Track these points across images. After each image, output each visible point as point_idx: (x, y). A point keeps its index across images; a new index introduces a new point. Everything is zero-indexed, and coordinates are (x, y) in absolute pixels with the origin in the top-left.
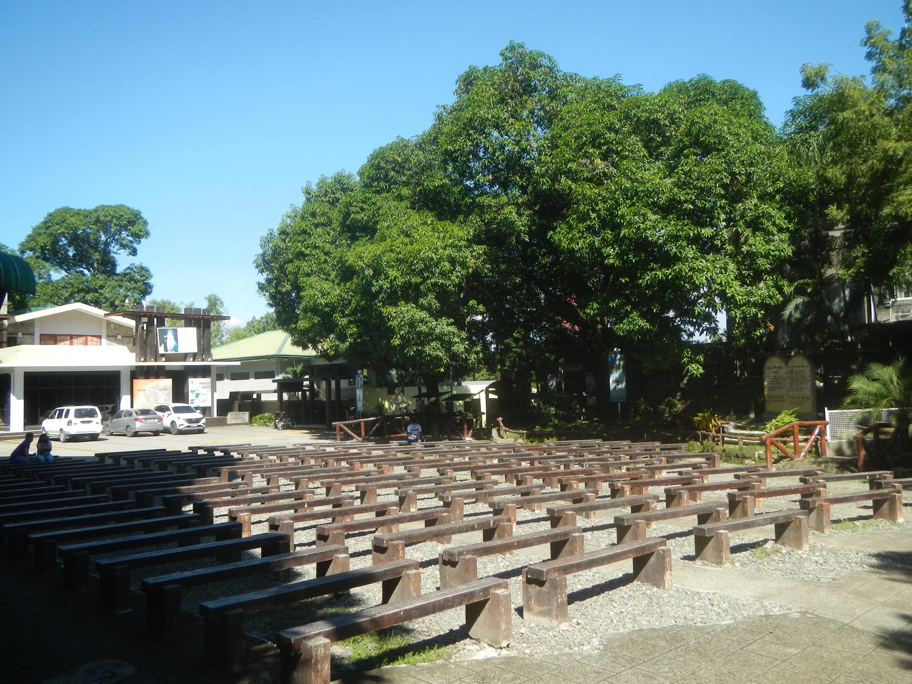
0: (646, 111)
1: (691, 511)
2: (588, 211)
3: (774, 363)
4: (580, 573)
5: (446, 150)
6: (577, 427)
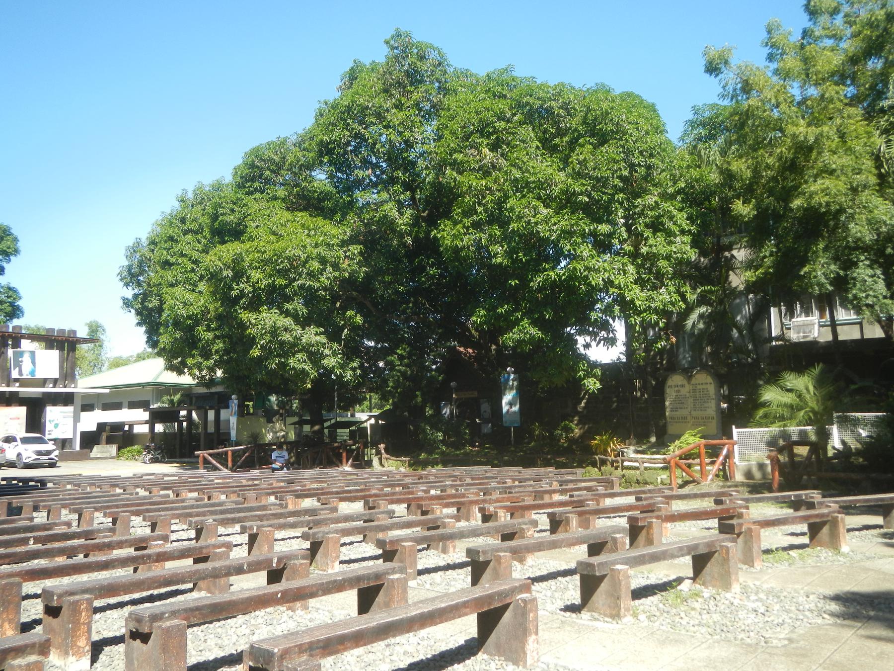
0: (539, 99)
1: (577, 538)
2: (474, 204)
3: (676, 380)
4: (398, 639)
5: (322, 141)
6: (466, 454)
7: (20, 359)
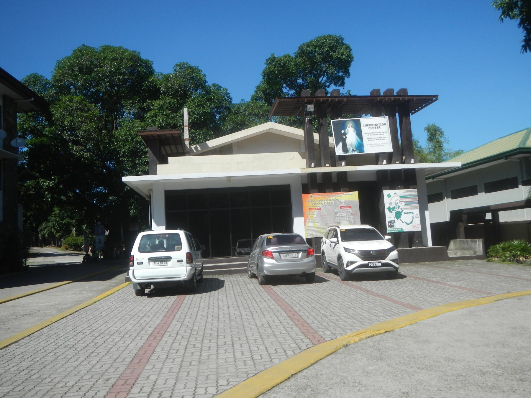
7: (343, 132)
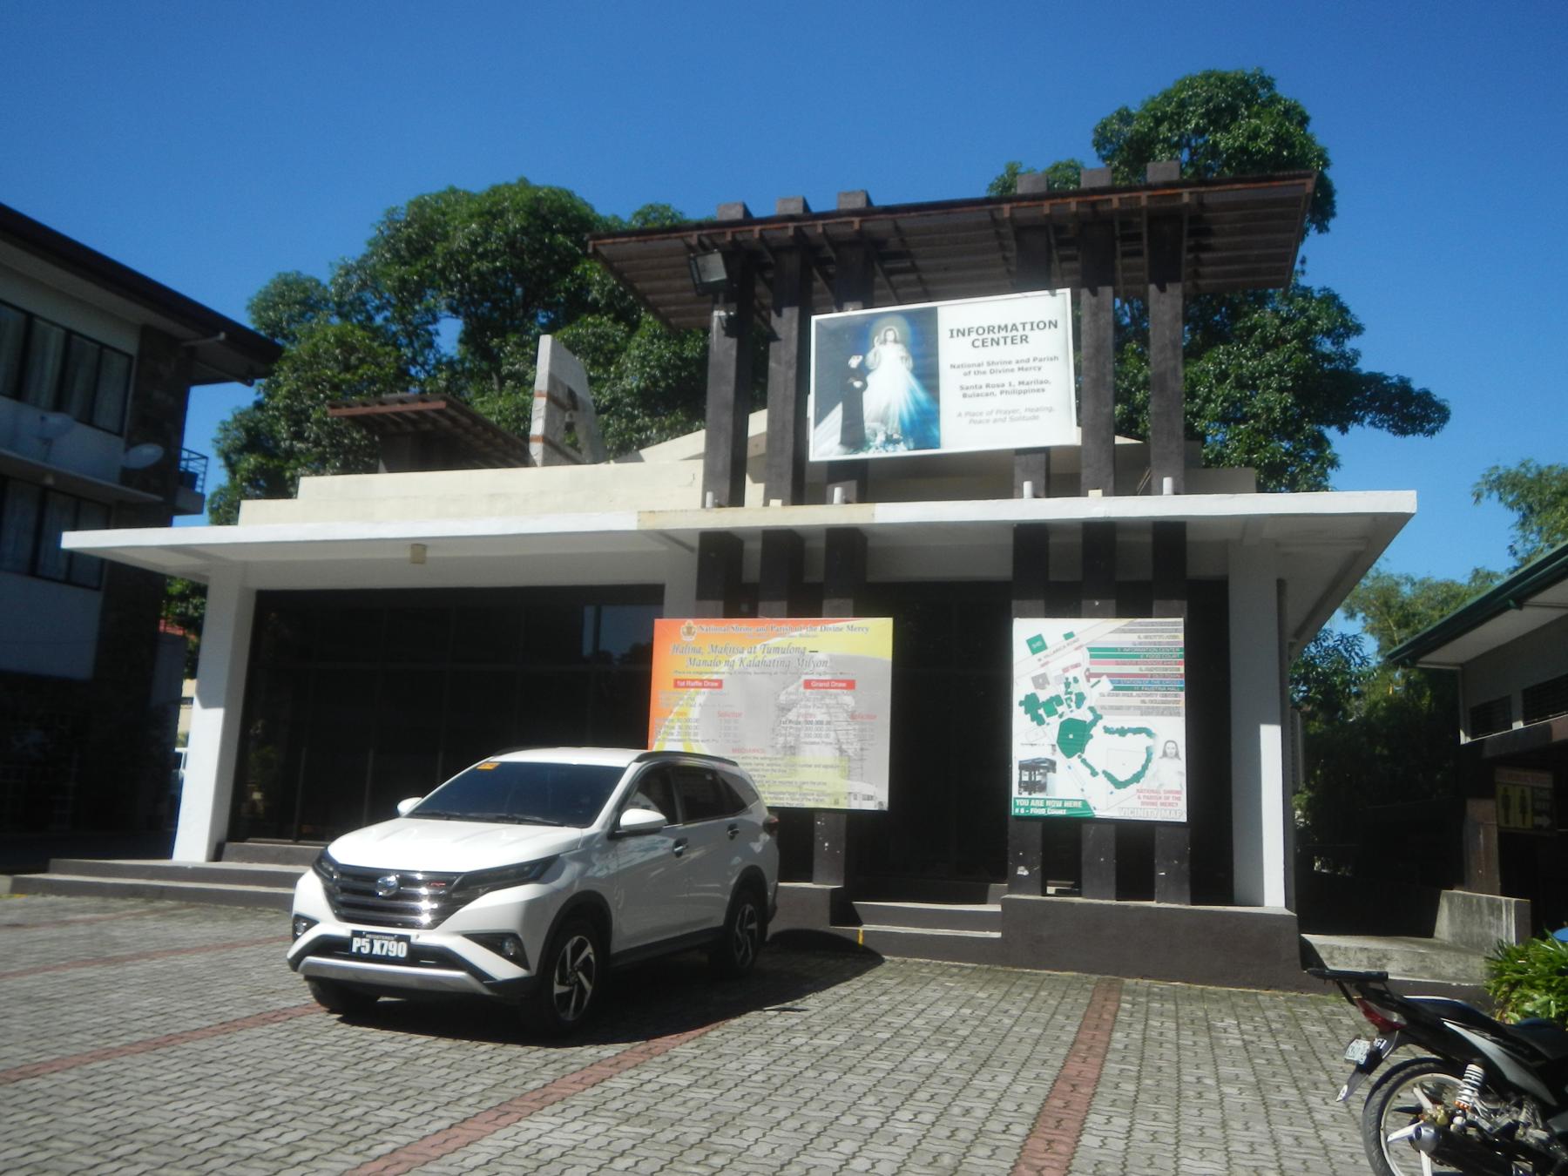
7: (854, 362)
